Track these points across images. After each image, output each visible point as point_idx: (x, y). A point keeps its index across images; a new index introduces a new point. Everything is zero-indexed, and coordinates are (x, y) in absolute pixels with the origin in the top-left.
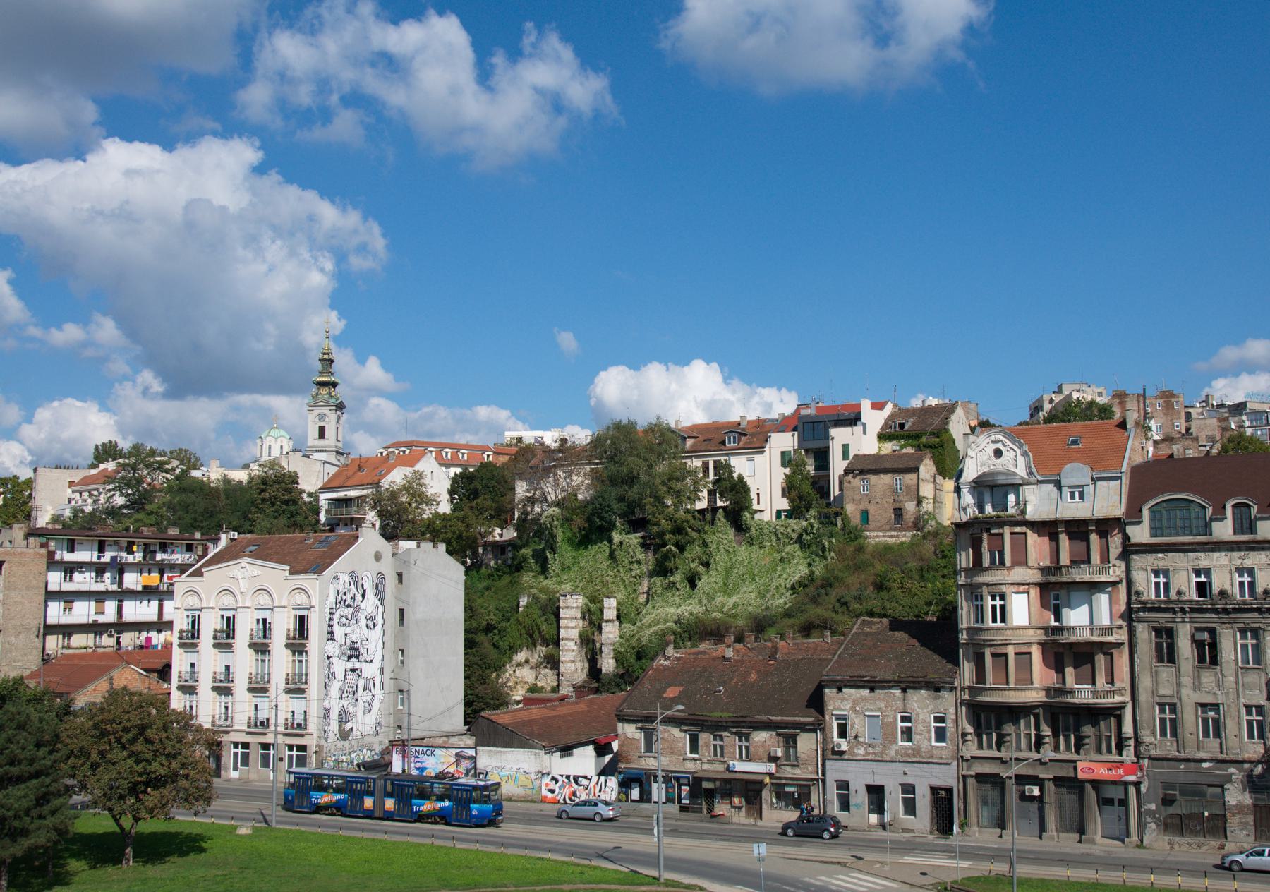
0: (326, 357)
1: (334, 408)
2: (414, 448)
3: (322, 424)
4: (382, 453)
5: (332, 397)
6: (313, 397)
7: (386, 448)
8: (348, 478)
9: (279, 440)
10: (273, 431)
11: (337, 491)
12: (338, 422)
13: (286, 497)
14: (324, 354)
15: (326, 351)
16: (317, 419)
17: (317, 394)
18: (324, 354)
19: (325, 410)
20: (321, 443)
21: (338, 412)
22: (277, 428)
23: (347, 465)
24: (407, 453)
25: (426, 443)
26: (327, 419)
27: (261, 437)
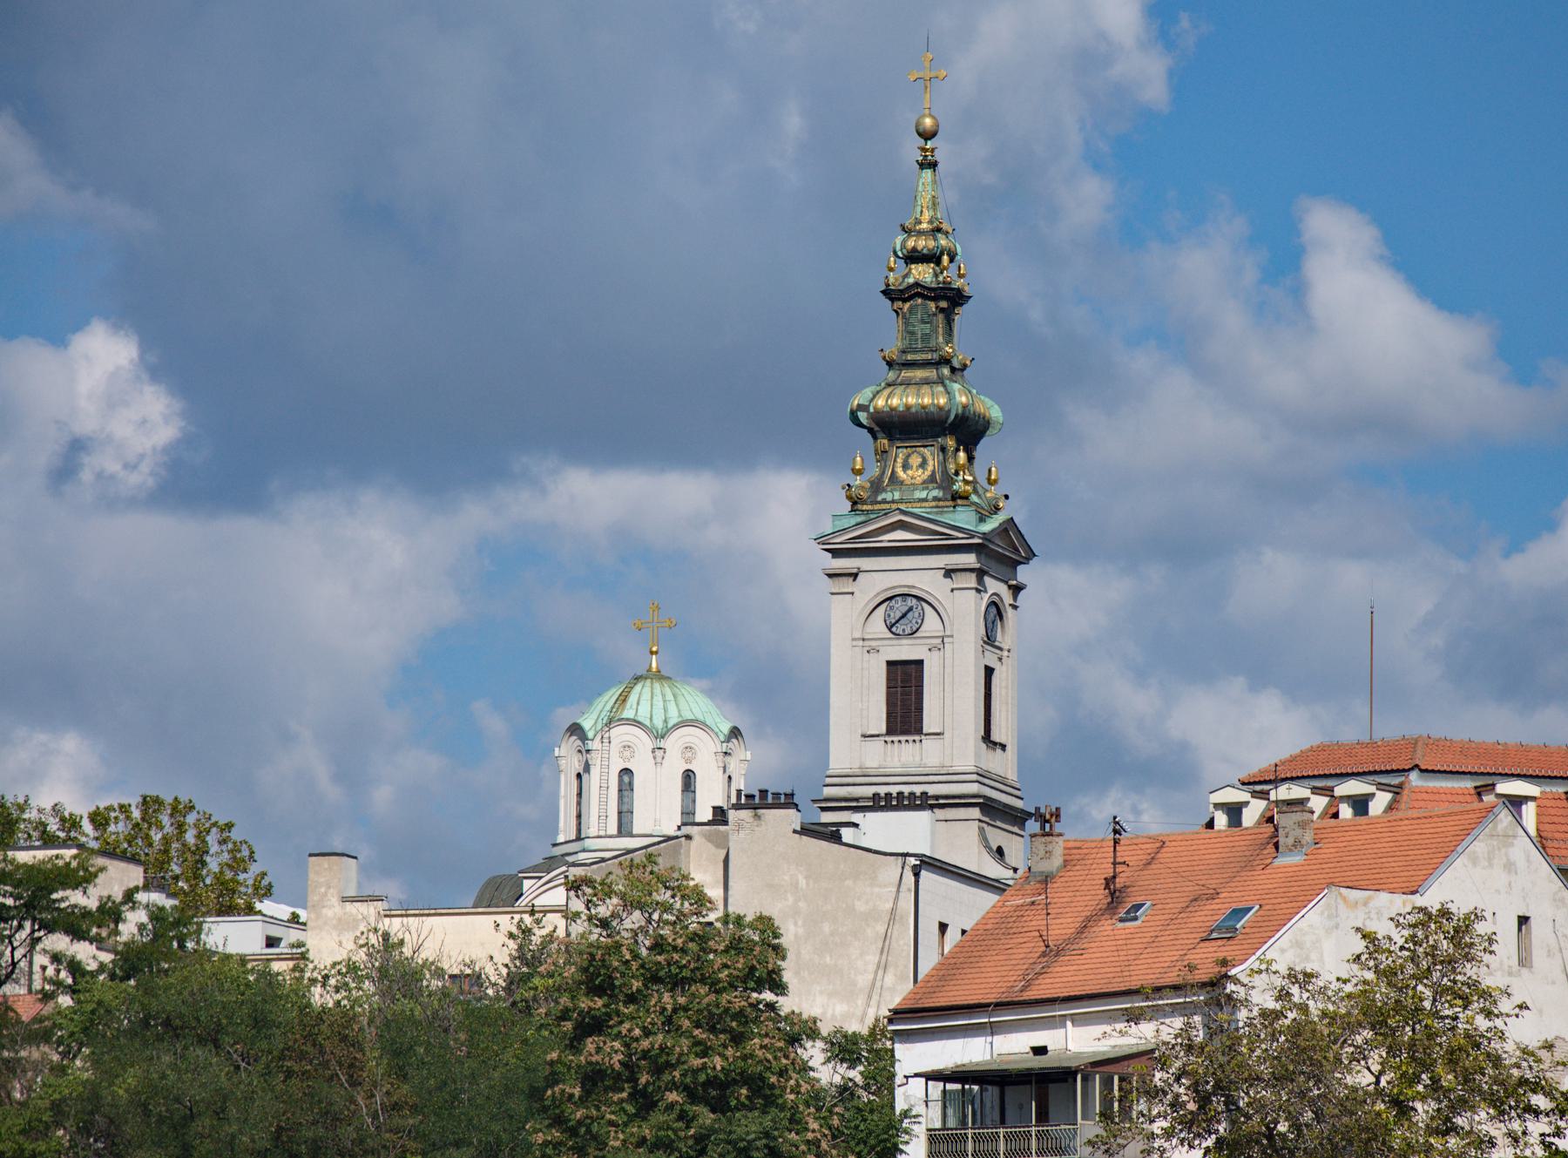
0: (923, 273)
1: (970, 559)
2: (1414, 776)
3: (905, 651)
4: (1234, 811)
5: (956, 497)
6: (855, 502)
7: (1258, 785)
8: (1051, 953)
9: (674, 743)
10: (641, 691)
11: (993, 1029)
12: (989, 640)
13: (718, 1062)
14: (913, 257)
15: (922, 244)
16: (878, 626)
17: (876, 486)
18: (913, 257)
19: (923, 575)
20: (904, 757)
21: (993, 586)
22: (659, 676)
23: (1046, 879)
24: (1379, 803)
25: (1483, 751)
26: (931, 624)
27: (576, 730)
